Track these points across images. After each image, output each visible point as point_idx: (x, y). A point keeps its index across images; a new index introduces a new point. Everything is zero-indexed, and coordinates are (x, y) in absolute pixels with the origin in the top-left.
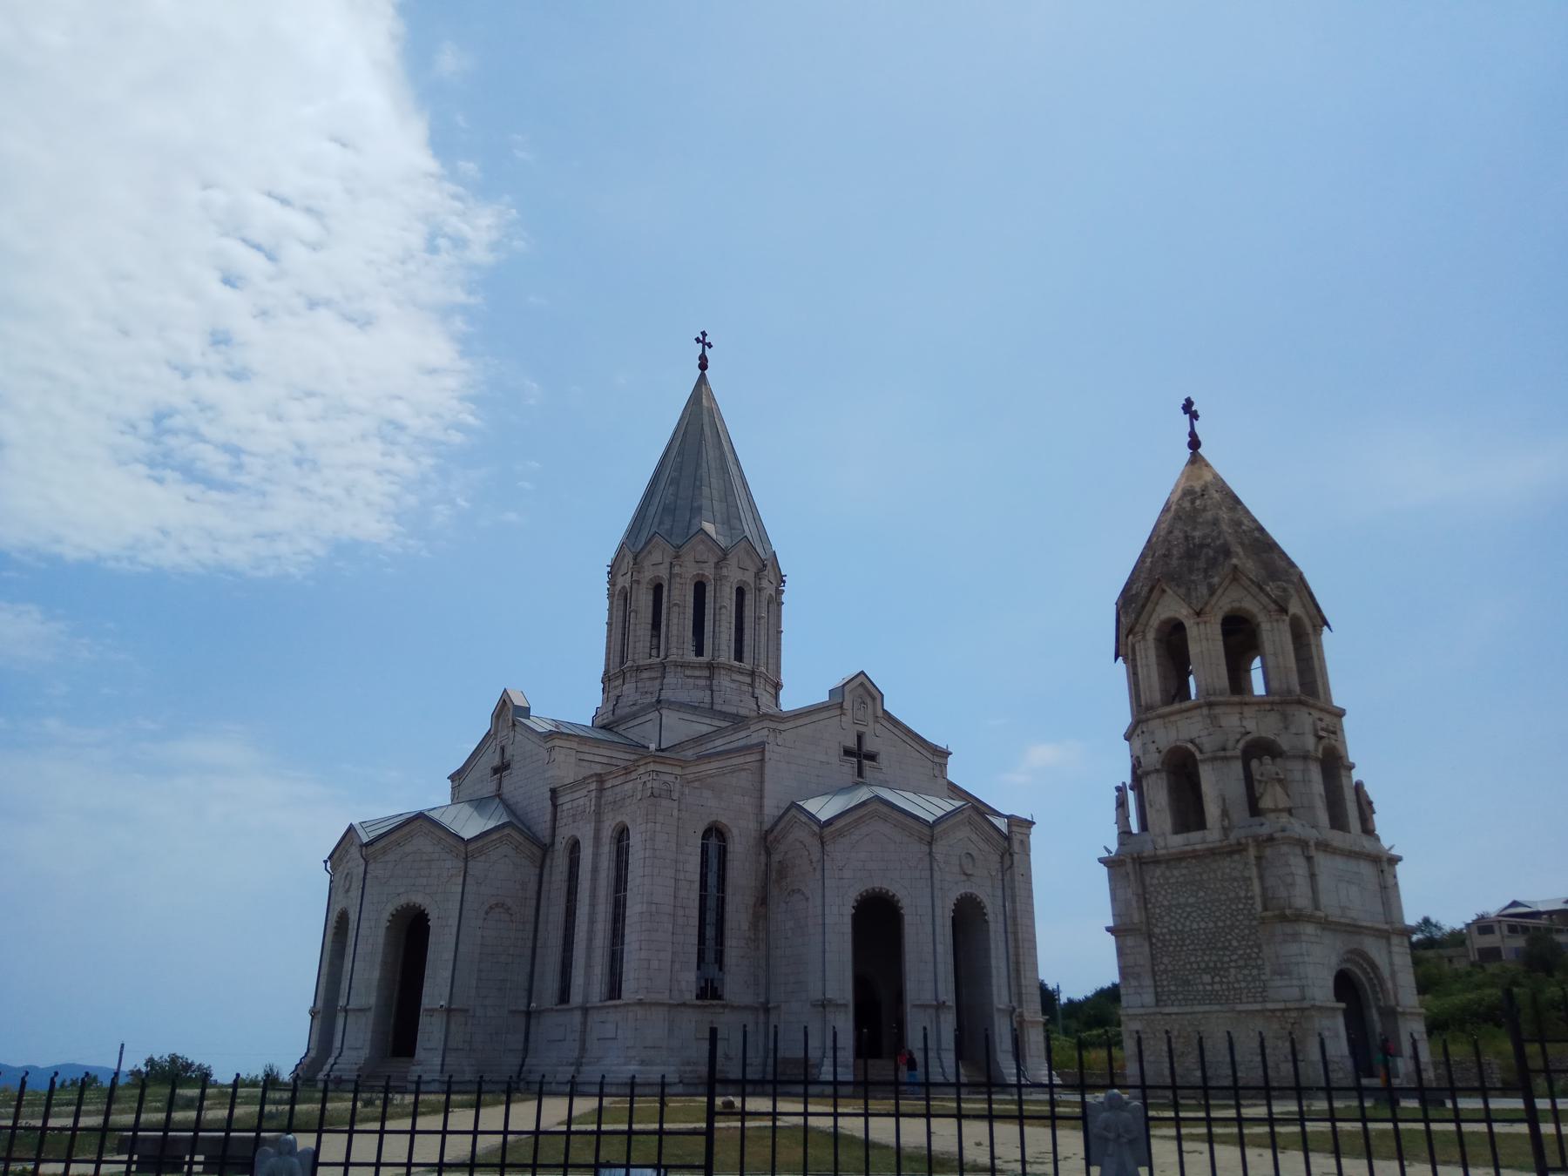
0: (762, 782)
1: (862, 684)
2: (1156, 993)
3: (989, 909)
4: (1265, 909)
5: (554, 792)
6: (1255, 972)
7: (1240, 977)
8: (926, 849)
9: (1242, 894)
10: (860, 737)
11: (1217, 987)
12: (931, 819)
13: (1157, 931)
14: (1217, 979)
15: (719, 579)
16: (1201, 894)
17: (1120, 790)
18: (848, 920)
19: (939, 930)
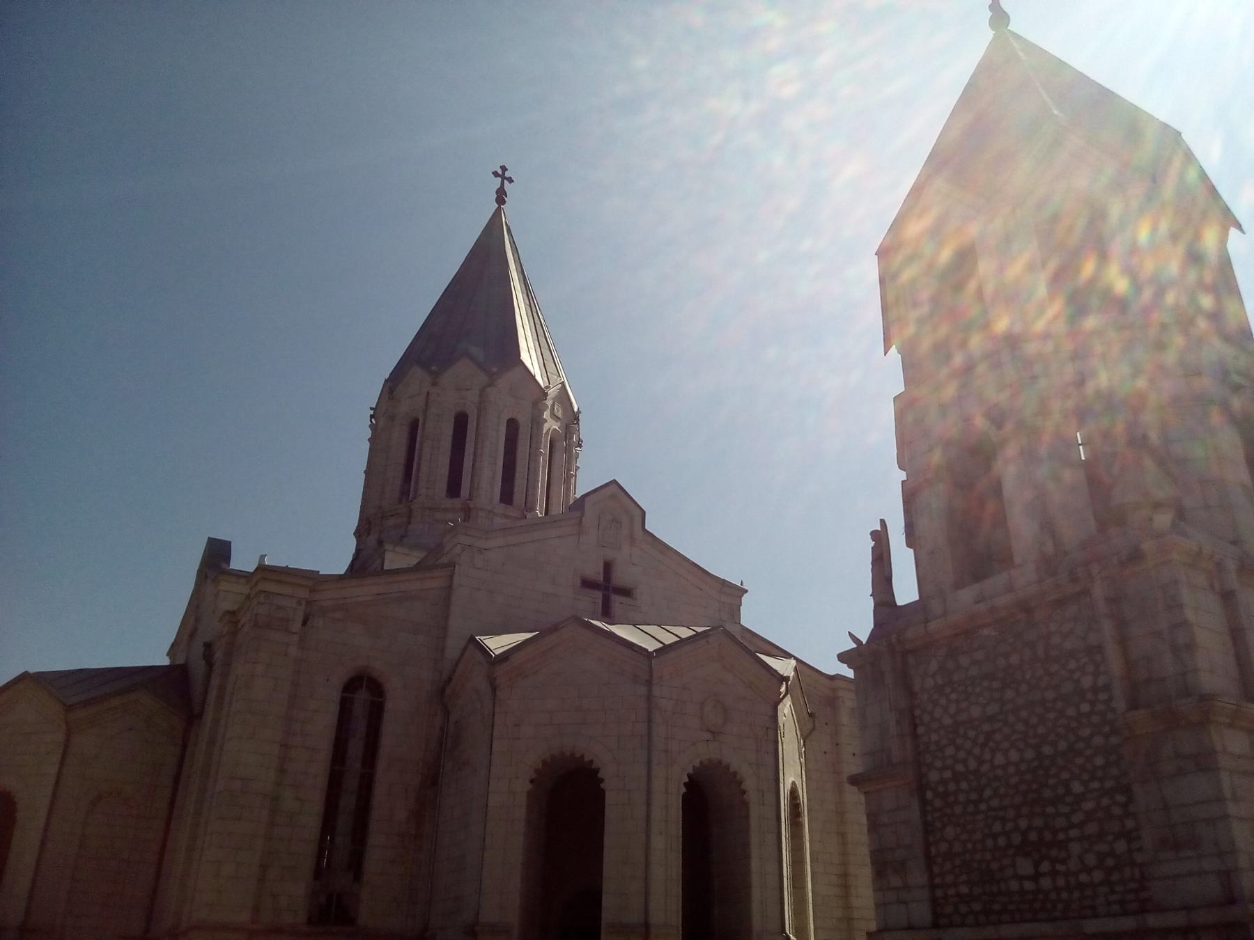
0: (446, 617)
1: (613, 496)
2: (934, 901)
3: (750, 784)
4: (1134, 705)
5: (208, 646)
6: (1121, 846)
7: (1091, 860)
8: (642, 690)
9: (1087, 682)
10: (608, 566)
11: (1046, 883)
12: (651, 646)
13: (934, 776)
14: (1045, 867)
15: (481, 406)
16: (1009, 694)
17: (880, 539)
18: (522, 799)
19: (657, 813)
